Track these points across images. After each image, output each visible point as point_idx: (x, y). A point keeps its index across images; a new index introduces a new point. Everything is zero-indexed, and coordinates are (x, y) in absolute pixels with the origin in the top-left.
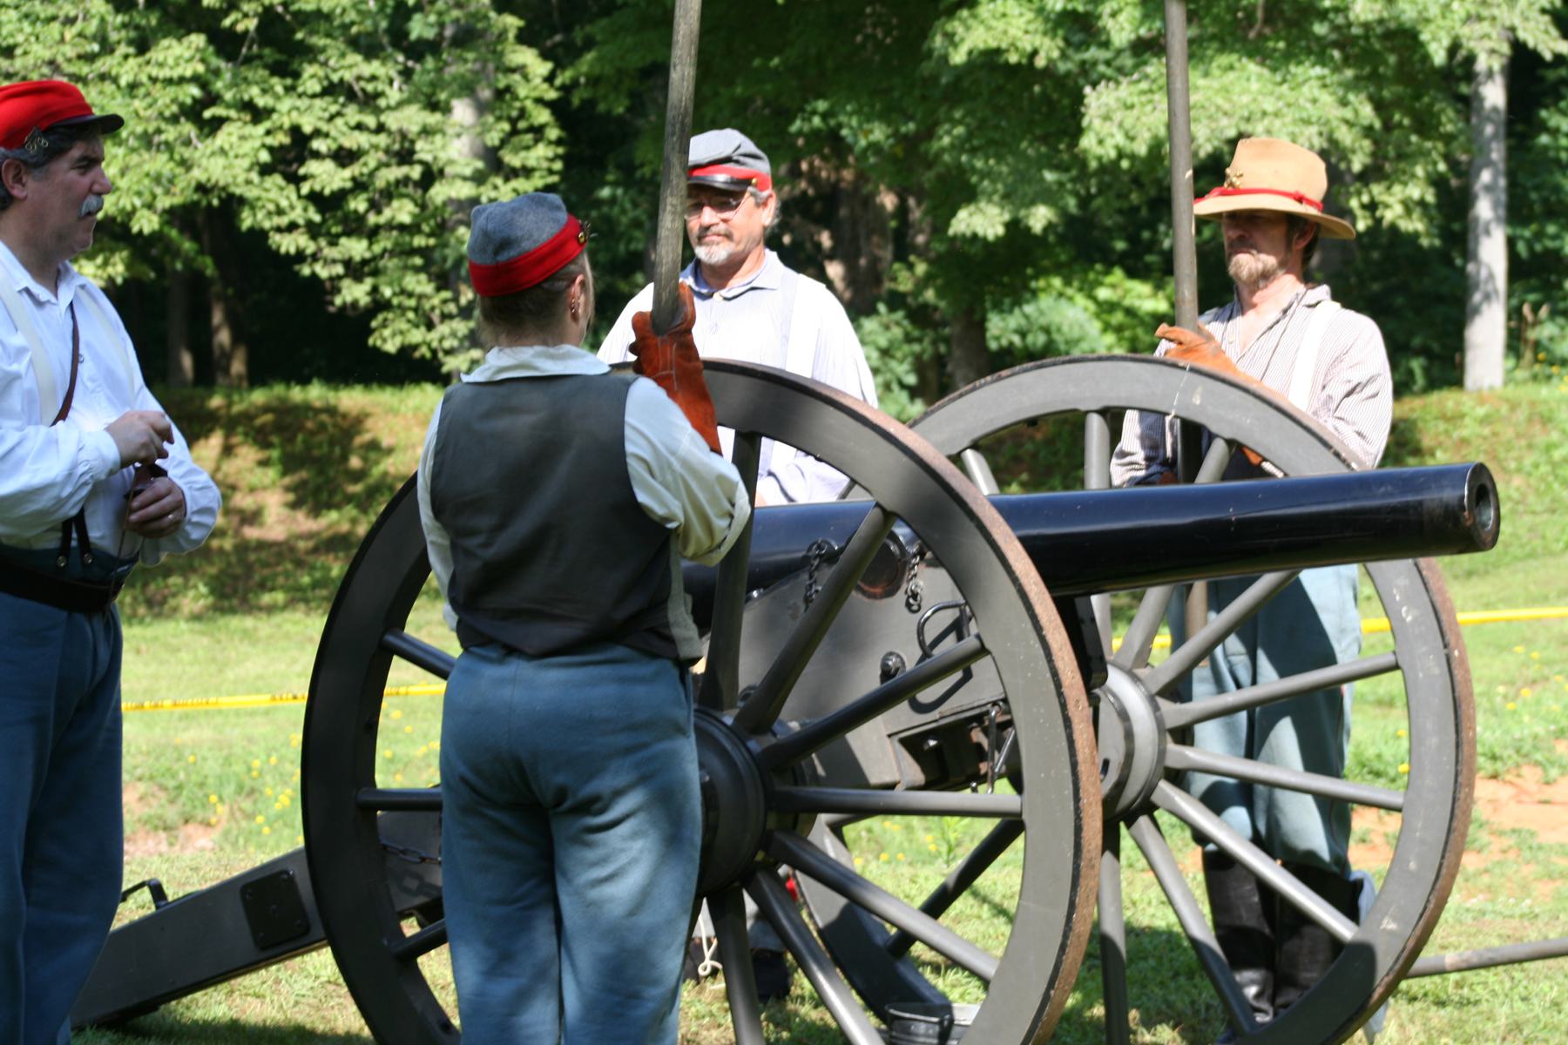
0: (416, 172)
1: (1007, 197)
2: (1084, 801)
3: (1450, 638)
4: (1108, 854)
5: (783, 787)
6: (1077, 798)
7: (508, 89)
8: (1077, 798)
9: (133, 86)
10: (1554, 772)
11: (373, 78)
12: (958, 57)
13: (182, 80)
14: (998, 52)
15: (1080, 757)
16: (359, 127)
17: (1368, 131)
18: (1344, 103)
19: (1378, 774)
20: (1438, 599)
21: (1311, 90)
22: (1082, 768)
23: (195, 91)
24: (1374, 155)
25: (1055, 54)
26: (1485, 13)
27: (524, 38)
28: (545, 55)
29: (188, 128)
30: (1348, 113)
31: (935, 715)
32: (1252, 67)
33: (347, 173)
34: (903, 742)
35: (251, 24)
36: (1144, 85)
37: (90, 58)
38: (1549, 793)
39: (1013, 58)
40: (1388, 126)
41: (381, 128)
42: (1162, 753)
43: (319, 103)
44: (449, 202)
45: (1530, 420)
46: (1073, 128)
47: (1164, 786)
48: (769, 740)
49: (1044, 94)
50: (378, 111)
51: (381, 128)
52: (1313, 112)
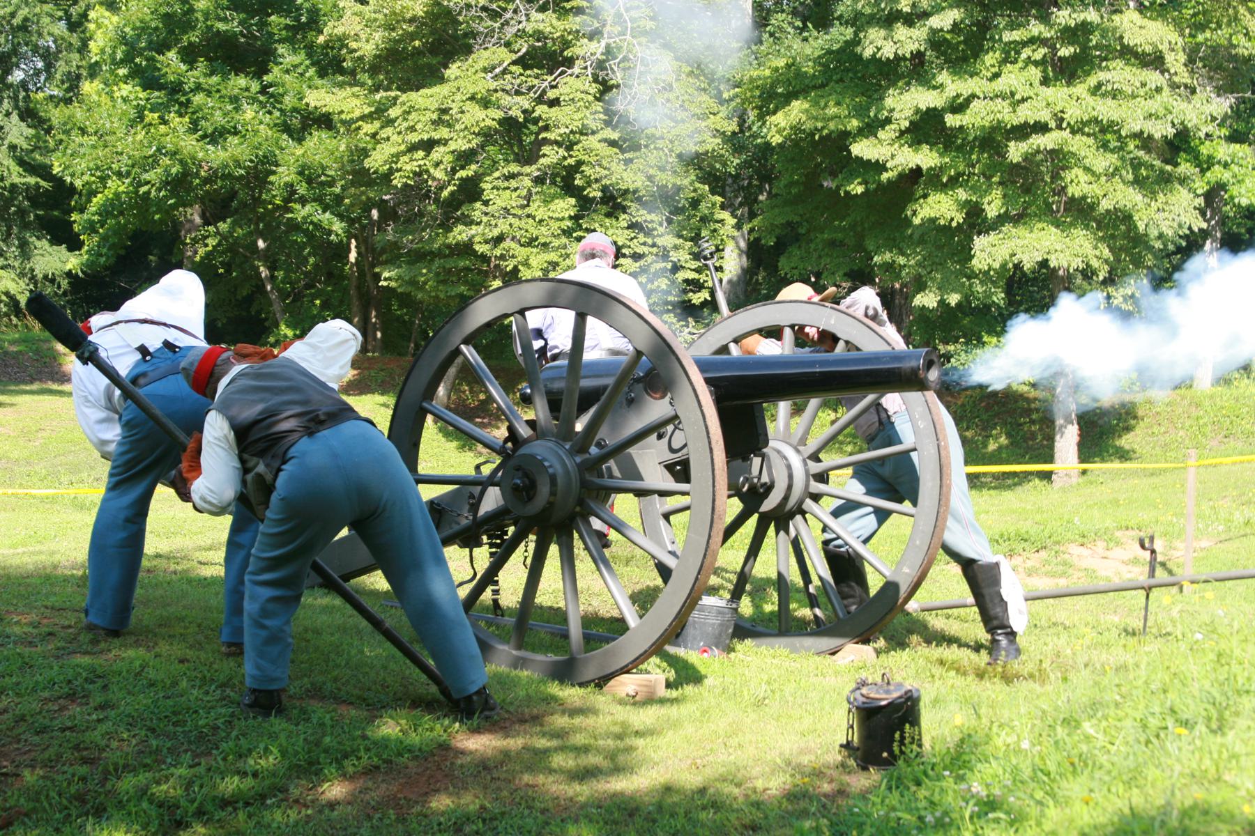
0: (669, 266)
1: (939, 288)
2: (717, 487)
3: (941, 437)
4: (782, 533)
5: (588, 477)
6: (714, 486)
7: (715, 230)
8: (714, 486)
9: (541, 221)
10: (1111, 545)
11: (652, 221)
12: (917, 221)
13: (563, 219)
14: (936, 219)
15: (716, 467)
16: (644, 244)
17: (1106, 261)
18: (1096, 248)
19: (1026, 541)
20: (936, 419)
21: (1081, 240)
22: (717, 472)
23: (569, 224)
24: (1110, 272)
25: (961, 221)
26: (1167, 208)
27: (723, 207)
28: (733, 215)
29: (564, 240)
30: (1098, 253)
31: (679, 454)
32: (1053, 229)
33: (637, 264)
34: (666, 467)
35: (599, 194)
36: (1001, 236)
37: (523, 207)
38: (1108, 554)
39: (942, 222)
40: (1118, 260)
41: (654, 245)
42: (807, 486)
43: (626, 231)
44: (687, 281)
45: (1190, 405)
46: (965, 254)
47: (809, 502)
48: (587, 456)
49: (960, 241)
50: (654, 237)
51: (654, 245)
52: (1080, 251)
